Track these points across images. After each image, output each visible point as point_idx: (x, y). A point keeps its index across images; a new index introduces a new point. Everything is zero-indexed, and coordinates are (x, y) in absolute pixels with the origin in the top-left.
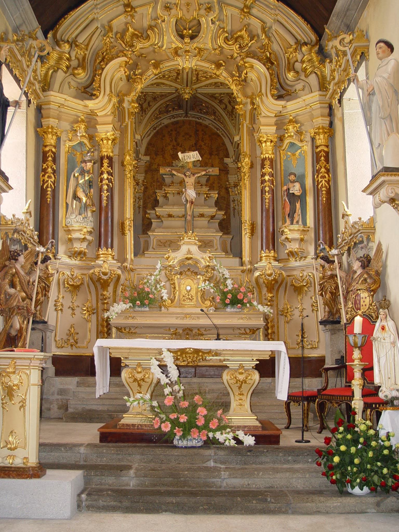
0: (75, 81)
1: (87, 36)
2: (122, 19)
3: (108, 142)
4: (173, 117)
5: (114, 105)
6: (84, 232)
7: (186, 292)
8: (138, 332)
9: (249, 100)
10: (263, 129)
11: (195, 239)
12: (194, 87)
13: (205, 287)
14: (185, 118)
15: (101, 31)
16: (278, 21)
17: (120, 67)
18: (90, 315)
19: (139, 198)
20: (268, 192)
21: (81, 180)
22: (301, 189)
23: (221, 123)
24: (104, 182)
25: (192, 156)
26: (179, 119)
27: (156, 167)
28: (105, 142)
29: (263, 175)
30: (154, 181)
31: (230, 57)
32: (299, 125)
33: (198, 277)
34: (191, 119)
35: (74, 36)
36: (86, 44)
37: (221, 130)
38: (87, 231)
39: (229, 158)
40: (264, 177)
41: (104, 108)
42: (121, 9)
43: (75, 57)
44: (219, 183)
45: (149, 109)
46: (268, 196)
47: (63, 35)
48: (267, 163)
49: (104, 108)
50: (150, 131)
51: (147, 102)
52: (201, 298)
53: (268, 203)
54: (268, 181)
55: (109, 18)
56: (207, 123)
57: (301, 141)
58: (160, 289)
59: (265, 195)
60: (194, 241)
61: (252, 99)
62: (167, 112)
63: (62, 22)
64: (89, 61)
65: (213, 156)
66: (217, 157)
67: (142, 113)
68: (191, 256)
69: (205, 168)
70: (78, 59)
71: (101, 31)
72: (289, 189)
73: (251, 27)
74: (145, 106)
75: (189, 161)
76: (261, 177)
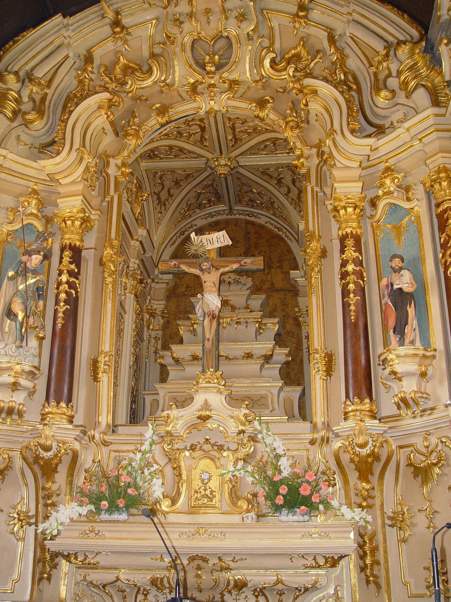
0: (27, 134)
1: (48, 69)
2: (110, 46)
3: (73, 222)
4: (211, 215)
5: (87, 168)
6: (16, 373)
7: (201, 484)
8: (102, 563)
9: (314, 150)
10: (341, 188)
11: (219, 383)
12: (233, 155)
13: (236, 473)
14: (229, 217)
15: (75, 62)
16: (354, 20)
17: (100, 107)
18: (22, 527)
19: (155, 338)
20: (353, 293)
21: (21, 284)
22: (414, 282)
23: (284, 219)
24: (61, 288)
25: (215, 239)
26: (220, 217)
27: (184, 289)
28: (69, 223)
29: (344, 264)
30: (180, 312)
31: (281, 90)
32: (402, 174)
33: (225, 454)
34: (237, 216)
35: (28, 67)
36: (48, 79)
37: (284, 230)
38: (23, 371)
39: (298, 269)
40: (345, 267)
41: (68, 171)
42: (107, 30)
43: (29, 98)
44: (283, 310)
45: (170, 200)
46: (353, 299)
47: (9, 65)
48: (350, 242)
49: (68, 171)
50: (175, 238)
51: (166, 190)
52: (230, 494)
53: (355, 311)
54: (353, 274)
55: (87, 45)
56: (262, 221)
57: (408, 199)
58: (149, 477)
59: (349, 297)
60: (217, 385)
61: (318, 146)
62: (200, 206)
63: (10, 47)
64: (52, 105)
65: (273, 270)
66: (279, 271)
67: (161, 208)
68: (208, 413)
69: (239, 259)
70: (34, 101)
71: (75, 62)
72: (392, 285)
73: (312, 41)
74: (164, 195)
75: (209, 247)
76: (341, 268)
